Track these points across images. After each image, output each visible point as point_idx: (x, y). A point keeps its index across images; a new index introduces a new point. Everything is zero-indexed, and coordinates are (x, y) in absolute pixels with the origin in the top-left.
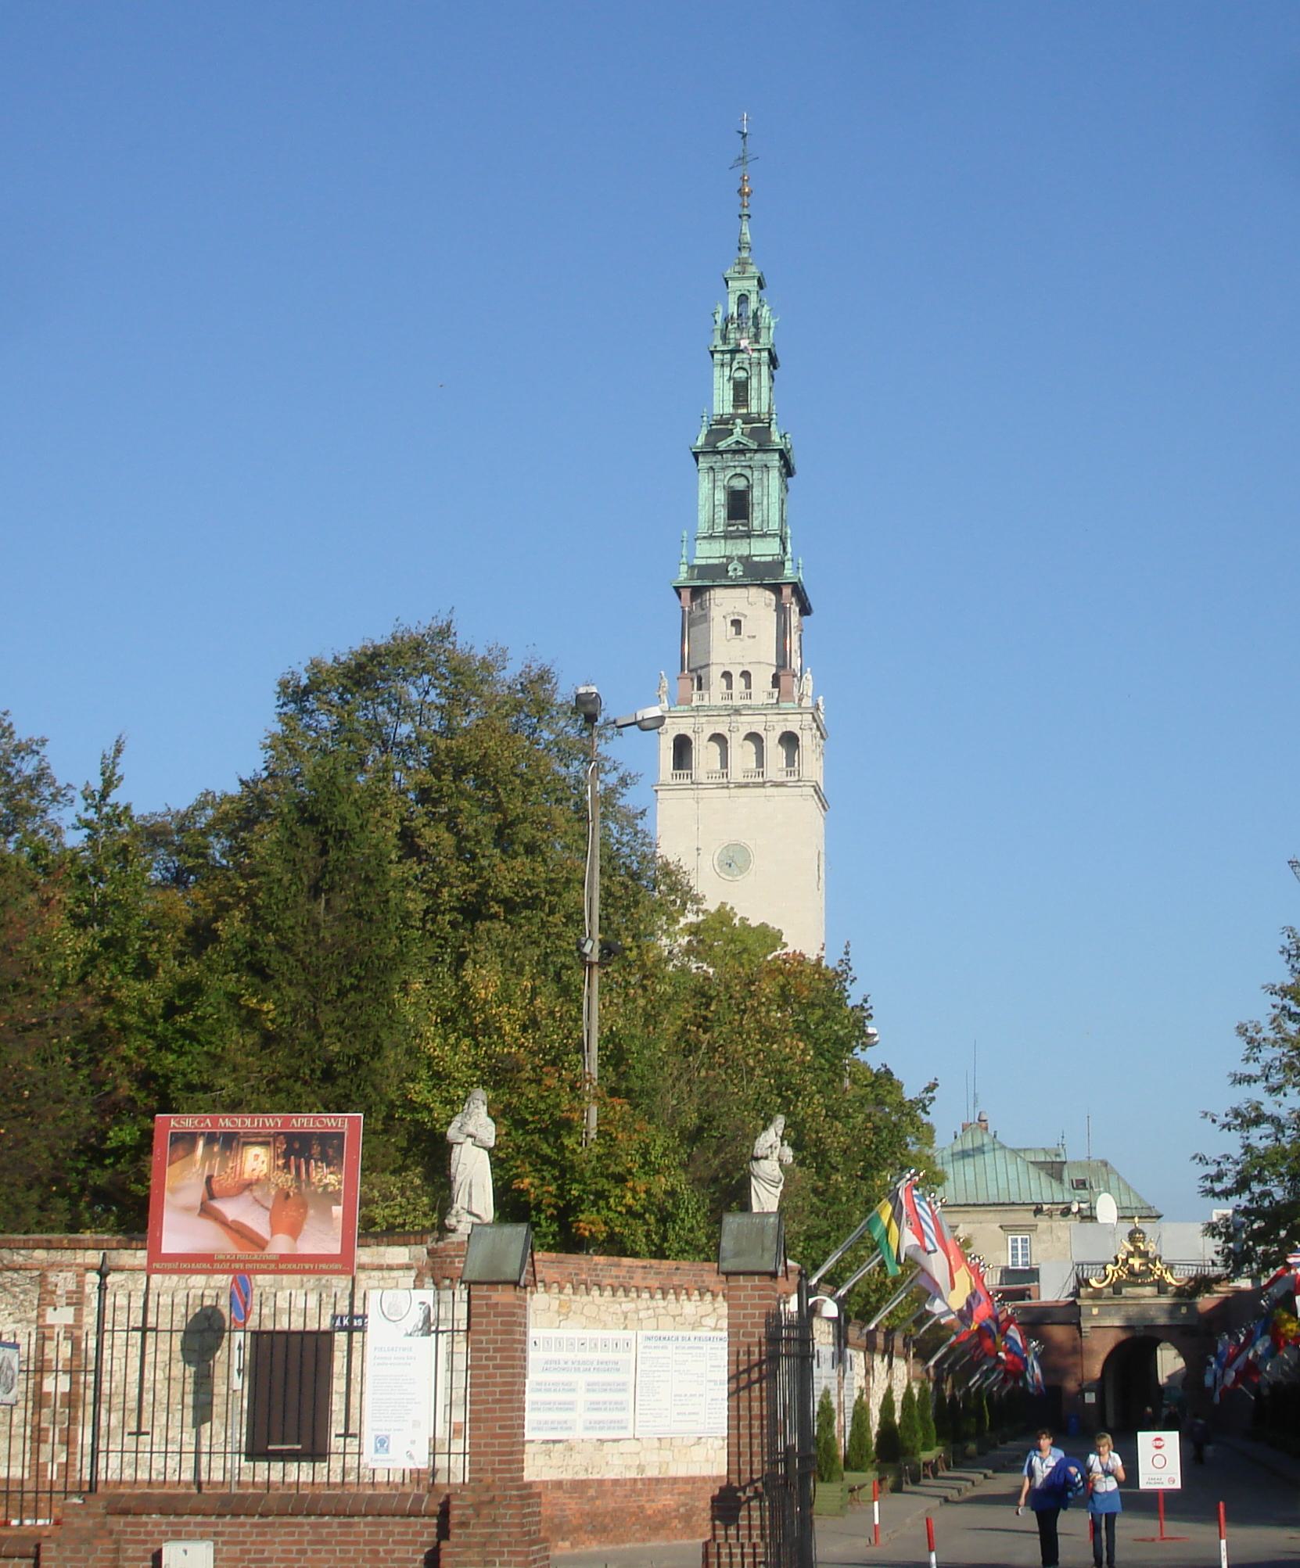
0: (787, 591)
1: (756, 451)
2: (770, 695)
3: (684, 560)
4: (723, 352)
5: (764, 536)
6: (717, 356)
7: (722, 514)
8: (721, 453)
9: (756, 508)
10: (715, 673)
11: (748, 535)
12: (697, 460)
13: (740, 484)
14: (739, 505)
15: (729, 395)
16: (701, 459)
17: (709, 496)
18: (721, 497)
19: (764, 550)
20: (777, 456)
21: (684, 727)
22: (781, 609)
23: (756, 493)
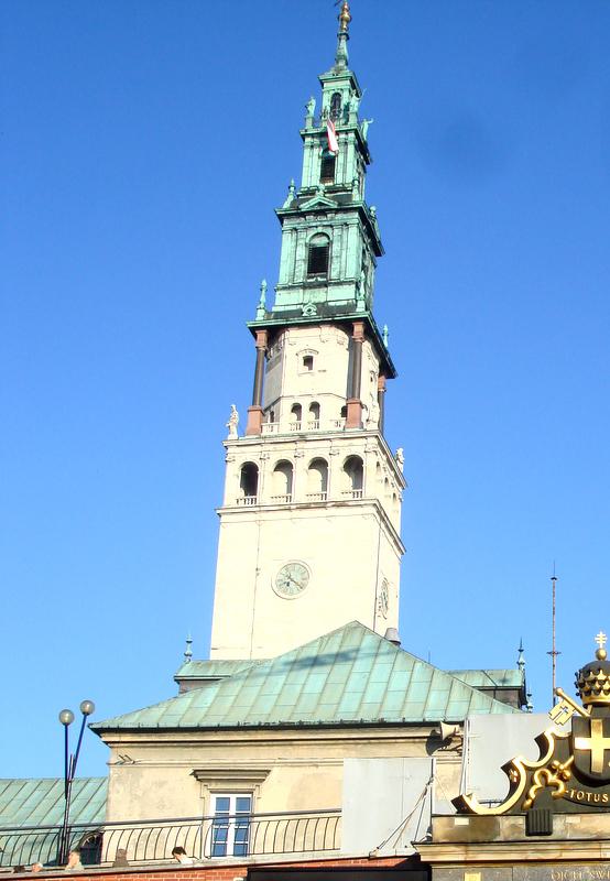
0: (359, 328)
1: (337, 211)
2: (338, 424)
3: (262, 305)
4: (312, 136)
5: (339, 283)
6: (308, 140)
7: (303, 267)
8: (303, 215)
9: (335, 260)
10: (285, 407)
11: (326, 285)
12: (282, 223)
13: (321, 242)
14: (318, 260)
15: (317, 171)
16: (285, 222)
17: (292, 253)
18: (302, 253)
19: (339, 296)
20: (356, 215)
21: (250, 455)
22: (354, 349)
23: (335, 248)
